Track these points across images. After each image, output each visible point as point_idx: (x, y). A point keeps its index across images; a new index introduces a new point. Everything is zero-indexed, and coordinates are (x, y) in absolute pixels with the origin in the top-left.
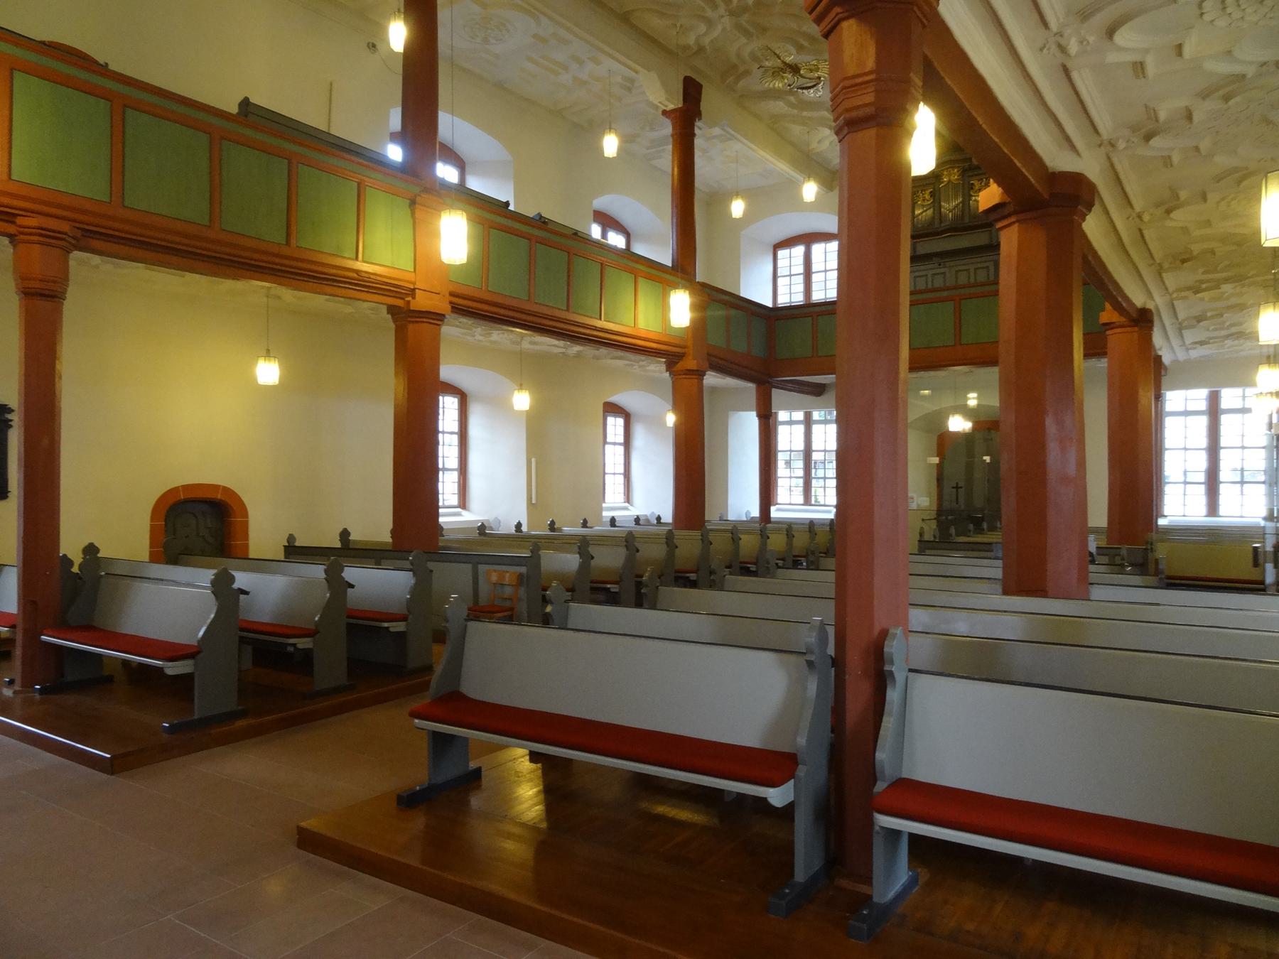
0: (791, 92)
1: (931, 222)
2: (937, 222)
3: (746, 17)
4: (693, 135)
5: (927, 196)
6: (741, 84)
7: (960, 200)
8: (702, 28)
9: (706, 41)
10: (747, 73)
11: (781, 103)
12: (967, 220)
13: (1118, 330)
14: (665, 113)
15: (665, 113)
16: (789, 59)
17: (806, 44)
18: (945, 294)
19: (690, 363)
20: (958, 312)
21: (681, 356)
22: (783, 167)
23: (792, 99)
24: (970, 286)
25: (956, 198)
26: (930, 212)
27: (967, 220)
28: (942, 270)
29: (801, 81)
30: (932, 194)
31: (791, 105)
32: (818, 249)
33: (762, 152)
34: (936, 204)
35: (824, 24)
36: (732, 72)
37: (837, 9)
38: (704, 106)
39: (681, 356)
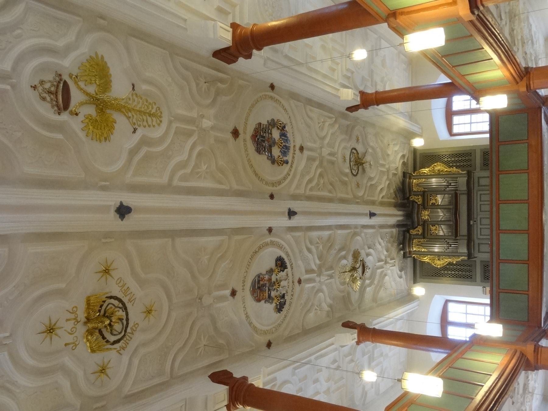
1: (449, 226)
2: (451, 223)
3: (323, 270)
4: (374, 329)
5: (434, 228)
6: (353, 301)
7: (439, 210)
8: (321, 294)
10: (349, 294)
11: (368, 289)
12: (451, 207)
13: (531, 82)
14: (358, 343)
15: (358, 343)
16: (348, 269)
17: (343, 253)
18: (494, 209)
19: (529, 349)
20: (506, 202)
21: (522, 355)
23: (367, 282)
24: (491, 194)
25: (438, 212)
26: (443, 226)
27: (451, 207)
28: (479, 219)
31: (370, 285)
32: (451, 318)
33: (392, 314)
34: (439, 223)
36: (346, 300)
38: (359, 322)
39: (522, 355)
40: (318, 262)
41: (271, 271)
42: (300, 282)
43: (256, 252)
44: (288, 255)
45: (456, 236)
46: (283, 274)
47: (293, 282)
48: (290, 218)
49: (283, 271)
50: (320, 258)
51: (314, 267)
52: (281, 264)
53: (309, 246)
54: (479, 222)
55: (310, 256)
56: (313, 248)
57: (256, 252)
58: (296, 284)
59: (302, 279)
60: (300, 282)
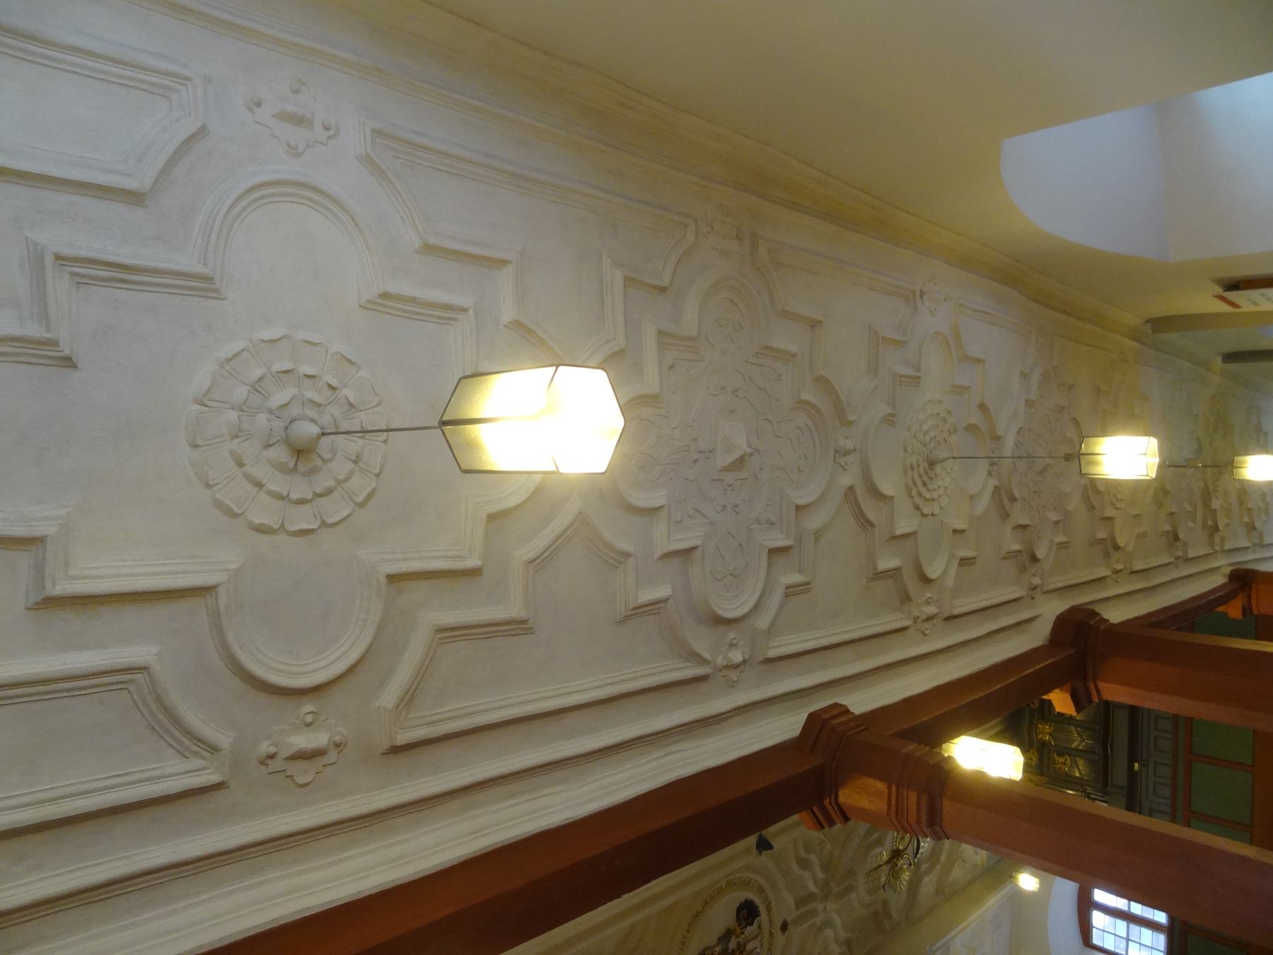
0: (918, 866)
5: (1062, 760)
6: (894, 913)
7: (1073, 728)
8: (829, 933)
9: (842, 934)
10: (885, 903)
11: (926, 879)
13: (1254, 602)
16: (885, 857)
17: (876, 835)
22: (993, 902)
23: (924, 867)
26: (1081, 762)
29: (910, 851)
30: (1061, 755)
31: (931, 869)
33: (972, 918)
35: (836, 818)
37: (826, 802)
40: (821, 875)
41: (728, 935)
42: (784, 927)
43: (698, 914)
44: (761, 890)
45: (1105, 783)
46: (750, 930)
47: (771, 934)
48: (760, 853)
49: (751, 924)
50: (825, 868)
51: (813, 889)
52: (747, 912)
53: (803, 854)
54: (1151, 768)
55: (807, 875)
56: (813, 858)
57: (698, 914)
58: (778, 933)
59: (789, 920)
60: (784, 927)
